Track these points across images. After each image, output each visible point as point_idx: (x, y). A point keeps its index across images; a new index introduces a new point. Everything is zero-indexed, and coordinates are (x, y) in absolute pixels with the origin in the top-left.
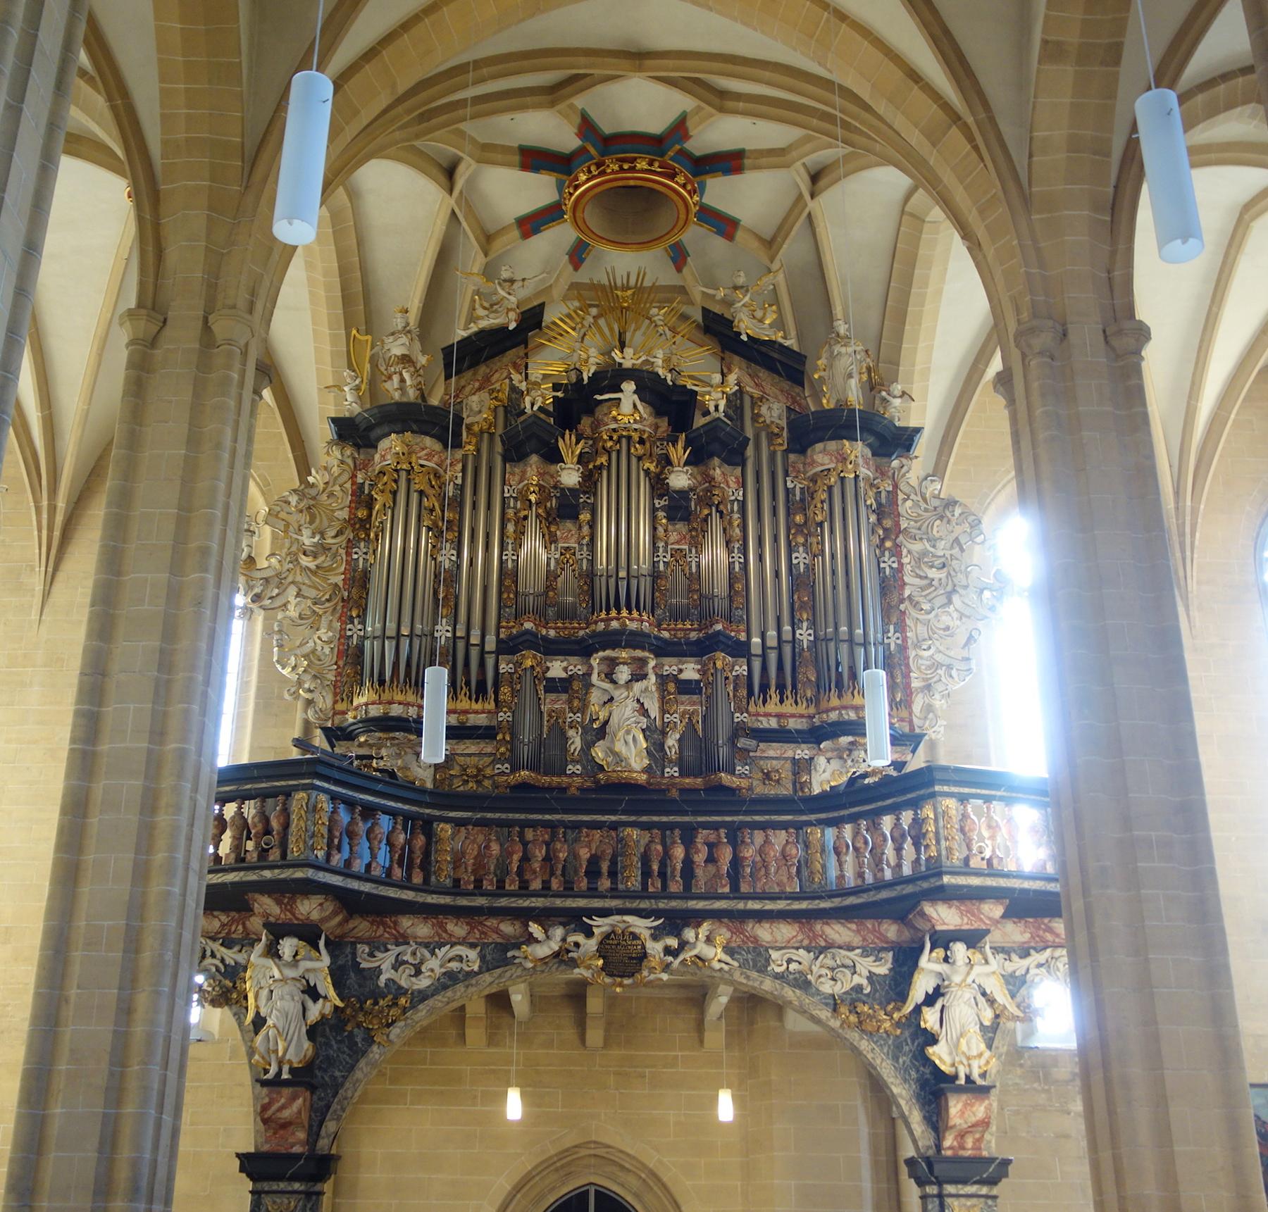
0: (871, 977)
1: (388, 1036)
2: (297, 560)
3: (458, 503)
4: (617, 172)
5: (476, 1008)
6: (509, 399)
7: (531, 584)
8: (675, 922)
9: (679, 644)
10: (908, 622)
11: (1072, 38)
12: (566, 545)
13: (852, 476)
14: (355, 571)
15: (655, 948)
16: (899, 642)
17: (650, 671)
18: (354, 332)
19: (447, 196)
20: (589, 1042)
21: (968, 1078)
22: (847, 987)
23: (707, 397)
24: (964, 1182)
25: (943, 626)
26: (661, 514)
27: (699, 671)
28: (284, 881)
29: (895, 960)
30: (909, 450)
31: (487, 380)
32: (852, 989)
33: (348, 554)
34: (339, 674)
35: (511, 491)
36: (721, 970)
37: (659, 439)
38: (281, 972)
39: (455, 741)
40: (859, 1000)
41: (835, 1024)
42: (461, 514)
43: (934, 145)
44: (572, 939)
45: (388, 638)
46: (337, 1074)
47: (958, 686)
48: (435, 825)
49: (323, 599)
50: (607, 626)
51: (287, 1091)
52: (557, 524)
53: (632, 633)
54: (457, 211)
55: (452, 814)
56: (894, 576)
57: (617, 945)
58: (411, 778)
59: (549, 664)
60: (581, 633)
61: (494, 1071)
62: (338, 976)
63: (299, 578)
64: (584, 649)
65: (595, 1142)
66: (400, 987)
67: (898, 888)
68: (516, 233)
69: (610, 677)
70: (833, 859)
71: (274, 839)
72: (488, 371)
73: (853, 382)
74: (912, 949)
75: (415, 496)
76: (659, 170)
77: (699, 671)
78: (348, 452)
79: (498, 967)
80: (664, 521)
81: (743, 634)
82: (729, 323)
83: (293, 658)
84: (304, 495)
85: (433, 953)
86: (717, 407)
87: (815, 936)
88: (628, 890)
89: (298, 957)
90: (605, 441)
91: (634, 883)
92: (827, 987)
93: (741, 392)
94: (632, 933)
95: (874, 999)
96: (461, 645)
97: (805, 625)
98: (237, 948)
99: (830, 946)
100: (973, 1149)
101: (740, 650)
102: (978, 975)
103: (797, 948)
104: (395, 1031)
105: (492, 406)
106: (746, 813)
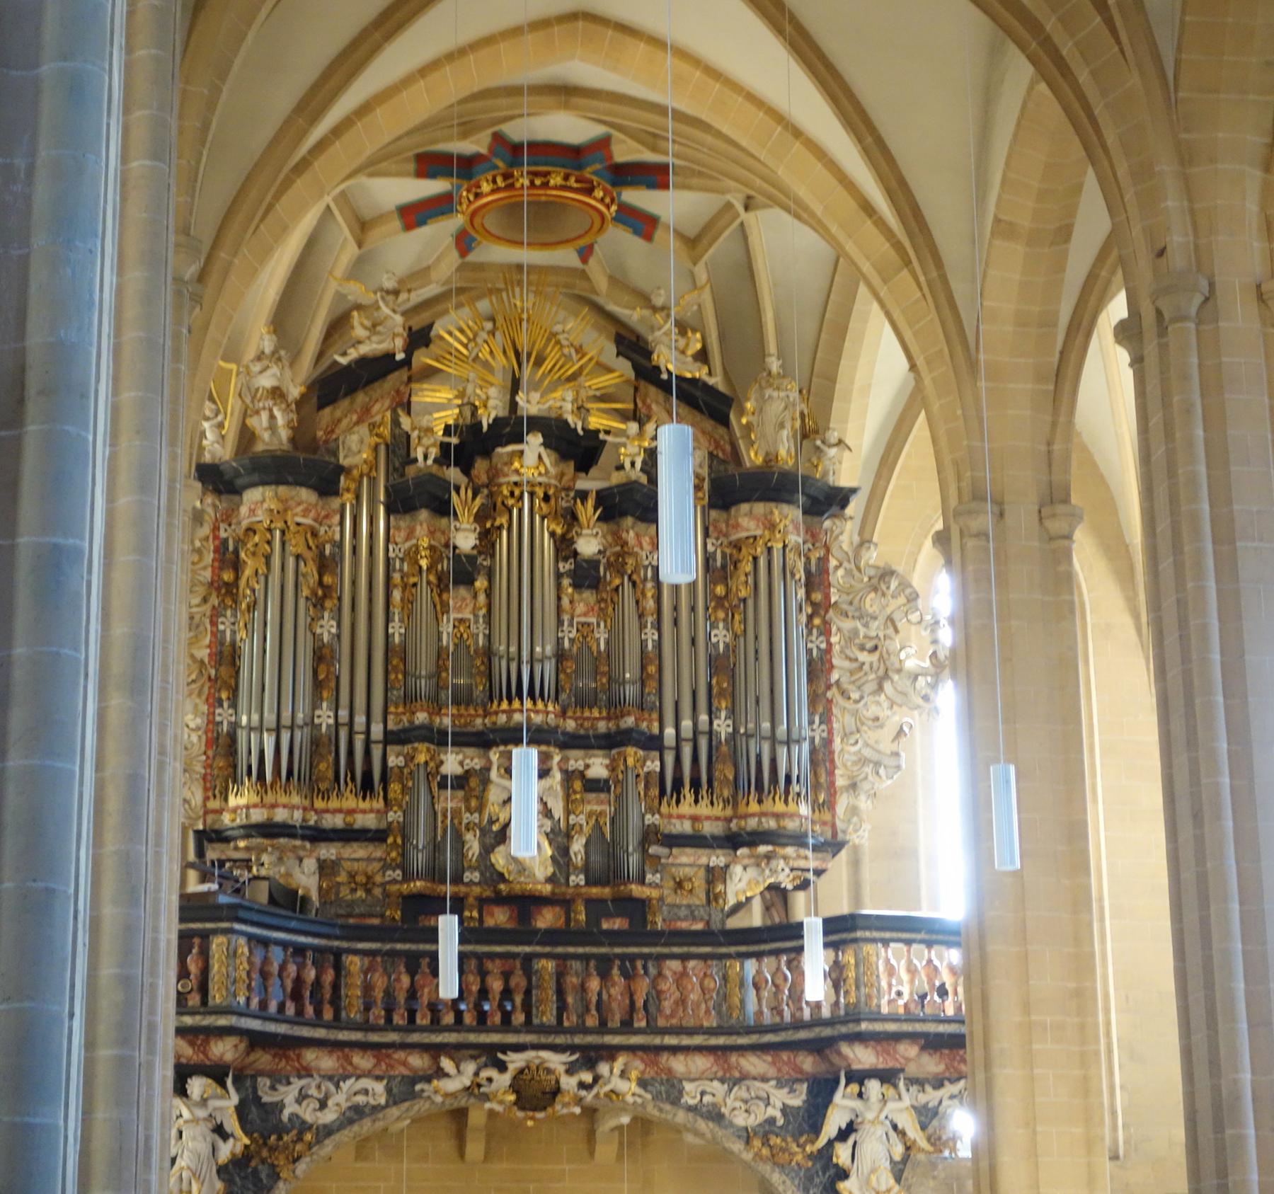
0: (785, 1110)
1: (294, 1172)
8: (590, 1057)
10: (835, 710)
11: (1025, 222)
12: (460, 616)
13: (780, 545)
14: (222, 644)
16: (825, 735)
22: (760, 1119)
23: (623, 450)
25: (872, 717)
26: (566, 582)
29: (810, 1091)
31: (366, 411)
33: (214, 623)
34: (207, 766)
35: (397, 551)
36: (635, 1102)
38: (191, 1112)
39: (339, 844)
40: (772, 1132)
41: (748, 1156)
44: (485, 1074)
47: (884, 785)
48: (344, 958)
50: (510, 718)
55: (361, 946)
56: (821, 659)
58: (294, 886)
62: (241, 1111)
64: (483, 741)
66: (304, 1122)
67: (817, 1030)
68: (397, 223)
70: (752, 993)
71: (192, 982)
72: (367, 399)
73: (785, 433)
74: (827, 1080)
75: (291, 562)
77: (607, 766)
80: (570, 590)
82: (648, 354)
85: (337, 1086)
86: (633, 464)
87: (730, 1068)
88: (542, 1025)
90: (506, 497)
91: (549, 1018)
92: (740, 1120)
95: (787, 1131)
97: (723, 714)
99: (744, 1077)
101: (653, 743)
102: (892, 1111)
103: (711, 1080)
104: (301, 1167)
105: (373, 444)
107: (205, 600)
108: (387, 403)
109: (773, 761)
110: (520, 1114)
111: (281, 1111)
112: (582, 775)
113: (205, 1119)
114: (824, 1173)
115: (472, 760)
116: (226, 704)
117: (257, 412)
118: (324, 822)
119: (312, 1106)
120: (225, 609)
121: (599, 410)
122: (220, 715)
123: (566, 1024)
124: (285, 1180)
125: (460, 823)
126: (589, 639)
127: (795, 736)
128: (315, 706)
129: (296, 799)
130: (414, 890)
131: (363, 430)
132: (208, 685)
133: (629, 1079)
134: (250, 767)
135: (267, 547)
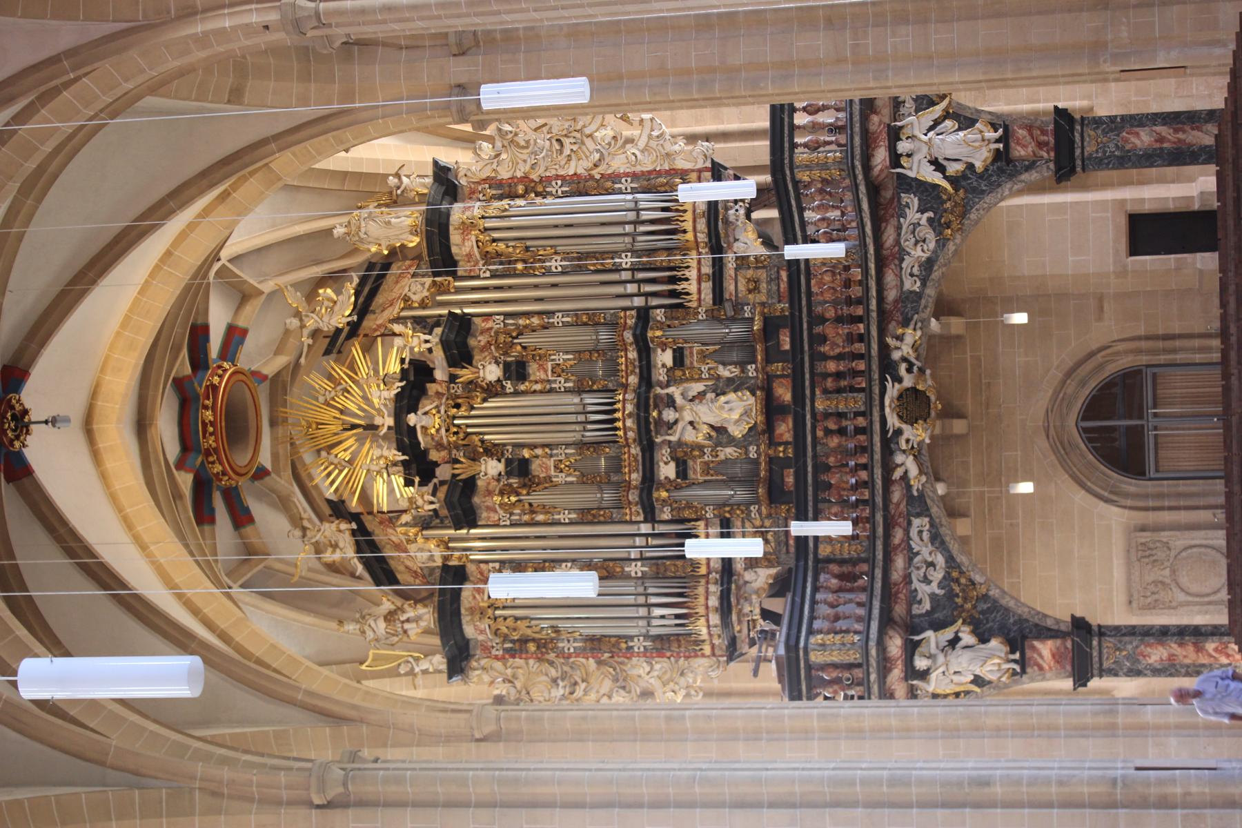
0: (922, 210)
1: (981, 584)
6: (415, 525)
7: (589, 497)
8: (888, 368)
9: (641, 367)
10: (610, 172)
12: (552, 468)
14: (584, 649)
15: (908, 381)
17: (666, 391)
21: (997, 141)
23: (416, 350)
24: (1072, 142)
26: (522, 387)
27: (663, 351)
28: (878, 663)
29: (907, 191)
30: (449, 169)
31: (398, 547)
32: (931, 225)
36: (921, 328)
44: (904, 446)
45: (649, 613)
46: (1011, 620)
48: (820, 557)
49: (614, 673)
50: (631, 429)
51: (1028, 653)
52: (534, 477)
53: (638, 406)
54: (240, 582)
58: (766, 586)
59: (662, 478)
61: (990, 510)
62: (938, 626)
64: (649, 448)
66: (944, 578)
67: (861, 196)
68: (248, 530)
69: (671, 426)
72: (388, 546)
77: (663, 351)
78: (474, 664)
80: (527, 384)
83: (667, 694)
85: (918, 553)
86: (427, 341)
88: (865, 403)
90: (458, 438)
92: (932, 245)
95: (939, 208)
96: (649, 553)
97: (617, 260)
101: (644, 315)
103: (901, 269)
104: (978, 578)
105: (422, 540)
107: (551, 663)
108: (390, 531)
109: (653, 222)
110: (933, 413)
111: (937, 595)
113: (946, 656)
117: (405, 632)
118: (716, 566)
119: (932, 572)
120: (558, 648)
121: (384, 363)
124: (988, 590)
127: (632, 205)
128: (628, 577)
130: (766, 496)
131: (412, 547)
132: (616, 659)
133: (903, 334)
134: (677, 625)
135: (508, 620)
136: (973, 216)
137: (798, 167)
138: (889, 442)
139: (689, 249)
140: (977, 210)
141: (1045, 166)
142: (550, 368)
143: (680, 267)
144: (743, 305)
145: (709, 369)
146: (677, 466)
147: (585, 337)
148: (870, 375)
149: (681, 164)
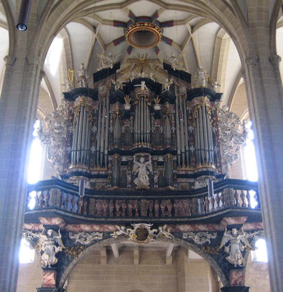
0: (211, 239)
2: (53, 130)
3: (97, 115)
4: (139, 26)
5: (104, 253)
6: (111, 87)
7: (116, 135)
10: (220, 145)
15: (151, 232)
18: (69, 70)
19: (94, 34)
20: (134, 263)
22: (204, 242)
26: (152, 117)
29: (218, 234)
30: (219, 99)
31: (105, 82)
32: (206, 242)
33: (67, 129)
34: (65, 161)
37: (152, 97)
39: (96, 179)
42: (98, 118)
43: (222, 12)
46: (64, 267)
48: (90, 199)
53: (145, 148)
54: (97, 38)
57: (140, 231)
59: (122, 158)
60: (131, 149)
62: (64, 240)
63: (54, 135)
64: (131, 153)
65: (137, 290)
66: (81, 244)
68: (113, 44)
69: (139, 161)
76: (151, 26)
77: (163, 159)
79: (108, 238)
80: (154, 119)
81: (175, 149)
84: (55, 114)
86: (167, 88)
87: (196, 229)
88: (143, 216)
89: (53, 235)
92: (199, 243)
93: (173, 84)
94: (144, 228)
96: (98, 153)
97: (192, 146)
98: (36, 233)
100: (239, 284)
101: (174, 153)
103: (191, 232)
106: (176, 195)
111: (75, 241)
112: (157, 161)
114: (223, 256)
115: (129, 158)
116: (69, 147)
117: (79, 82)
120: (70, 125)
122: (68, 149)
123: (150, 216)
125: (126, 173)
126: (158, 130)
127: (210, 149)
128: (91, 146)
129: (84, 167)
132: (65, 142)
136: (209, 257)
137: (228, 189)
138: (128, 225)
139: (195, 168)
140: (211, 259)
141: (227, 283)
142: (159, 126)
143: (190, 165)
144: (178, 184)
145: (157, 173)
146: (125, 162)
147: (168, 135)
148: (153, 218)
149: (224, 167)
